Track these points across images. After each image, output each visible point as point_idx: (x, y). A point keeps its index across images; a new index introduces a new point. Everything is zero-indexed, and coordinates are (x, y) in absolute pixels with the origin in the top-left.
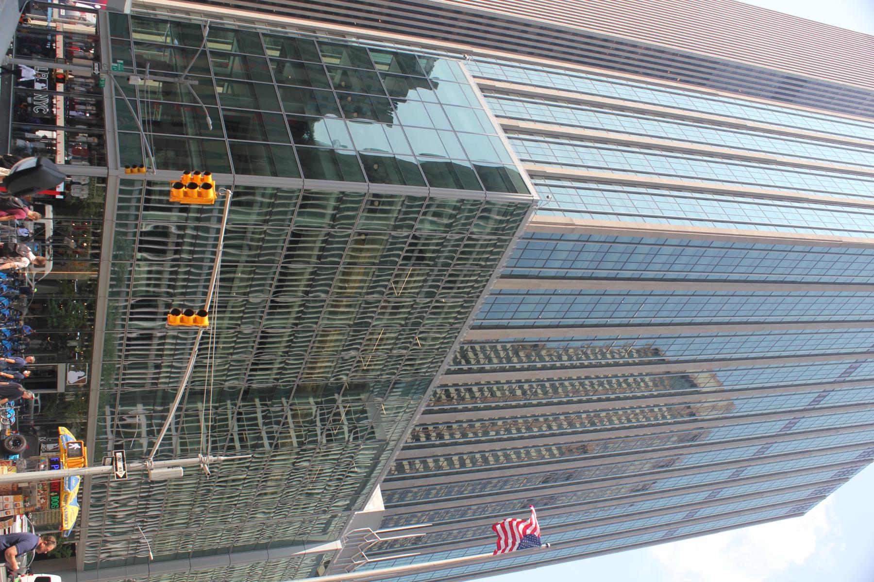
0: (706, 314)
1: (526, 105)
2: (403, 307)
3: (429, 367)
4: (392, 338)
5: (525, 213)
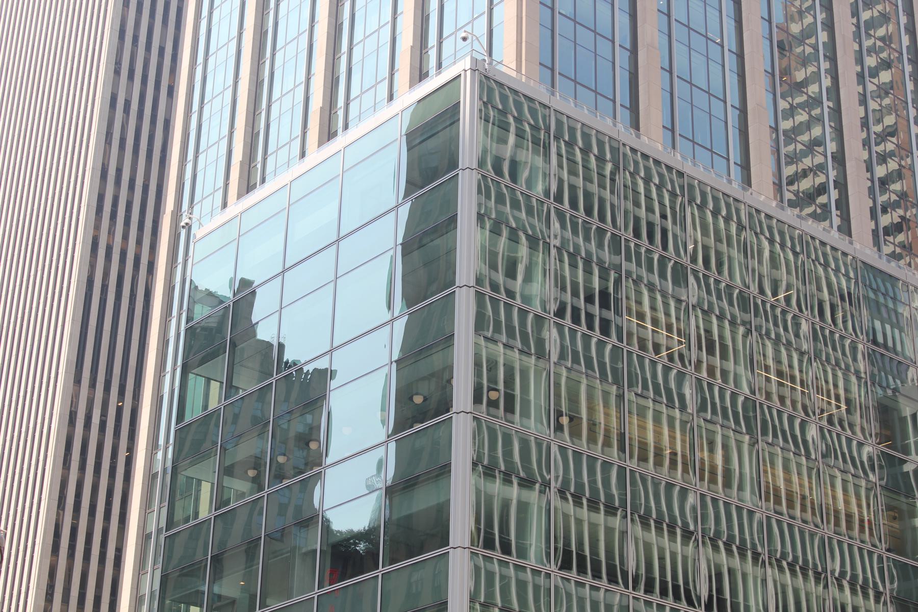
1: (276, 94)
2: (708, 332)
3: (837, 271)
4: (777, 352)
5: (501, 85)
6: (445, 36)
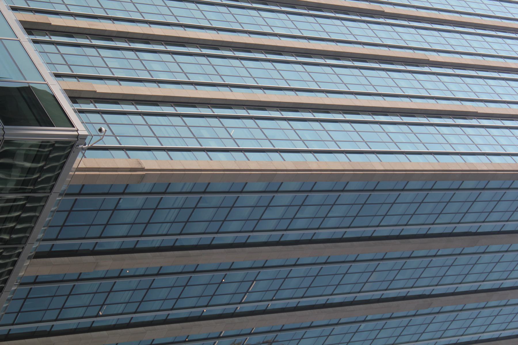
0: (348, 288)
5: (67, 156)
6: (104, 116)
